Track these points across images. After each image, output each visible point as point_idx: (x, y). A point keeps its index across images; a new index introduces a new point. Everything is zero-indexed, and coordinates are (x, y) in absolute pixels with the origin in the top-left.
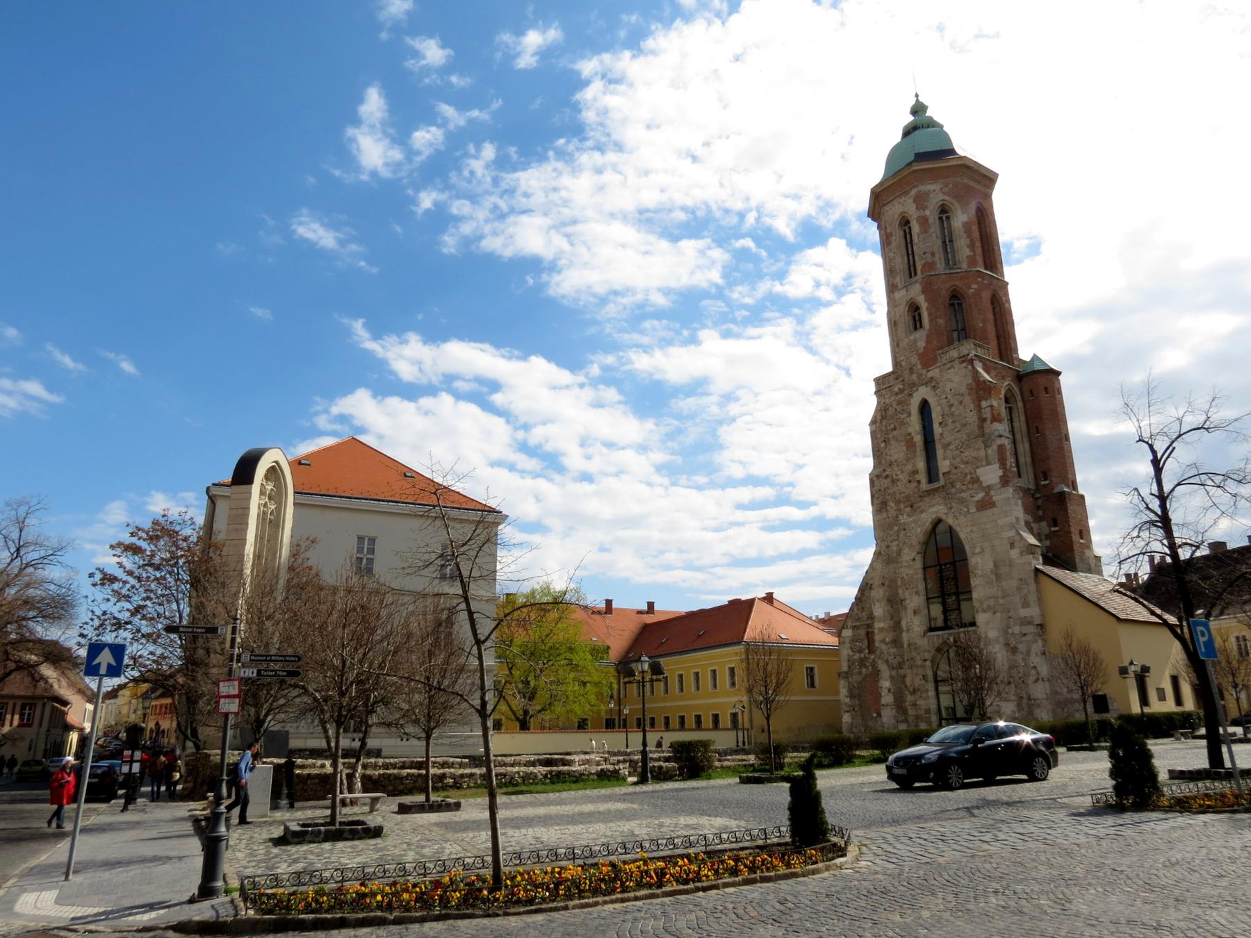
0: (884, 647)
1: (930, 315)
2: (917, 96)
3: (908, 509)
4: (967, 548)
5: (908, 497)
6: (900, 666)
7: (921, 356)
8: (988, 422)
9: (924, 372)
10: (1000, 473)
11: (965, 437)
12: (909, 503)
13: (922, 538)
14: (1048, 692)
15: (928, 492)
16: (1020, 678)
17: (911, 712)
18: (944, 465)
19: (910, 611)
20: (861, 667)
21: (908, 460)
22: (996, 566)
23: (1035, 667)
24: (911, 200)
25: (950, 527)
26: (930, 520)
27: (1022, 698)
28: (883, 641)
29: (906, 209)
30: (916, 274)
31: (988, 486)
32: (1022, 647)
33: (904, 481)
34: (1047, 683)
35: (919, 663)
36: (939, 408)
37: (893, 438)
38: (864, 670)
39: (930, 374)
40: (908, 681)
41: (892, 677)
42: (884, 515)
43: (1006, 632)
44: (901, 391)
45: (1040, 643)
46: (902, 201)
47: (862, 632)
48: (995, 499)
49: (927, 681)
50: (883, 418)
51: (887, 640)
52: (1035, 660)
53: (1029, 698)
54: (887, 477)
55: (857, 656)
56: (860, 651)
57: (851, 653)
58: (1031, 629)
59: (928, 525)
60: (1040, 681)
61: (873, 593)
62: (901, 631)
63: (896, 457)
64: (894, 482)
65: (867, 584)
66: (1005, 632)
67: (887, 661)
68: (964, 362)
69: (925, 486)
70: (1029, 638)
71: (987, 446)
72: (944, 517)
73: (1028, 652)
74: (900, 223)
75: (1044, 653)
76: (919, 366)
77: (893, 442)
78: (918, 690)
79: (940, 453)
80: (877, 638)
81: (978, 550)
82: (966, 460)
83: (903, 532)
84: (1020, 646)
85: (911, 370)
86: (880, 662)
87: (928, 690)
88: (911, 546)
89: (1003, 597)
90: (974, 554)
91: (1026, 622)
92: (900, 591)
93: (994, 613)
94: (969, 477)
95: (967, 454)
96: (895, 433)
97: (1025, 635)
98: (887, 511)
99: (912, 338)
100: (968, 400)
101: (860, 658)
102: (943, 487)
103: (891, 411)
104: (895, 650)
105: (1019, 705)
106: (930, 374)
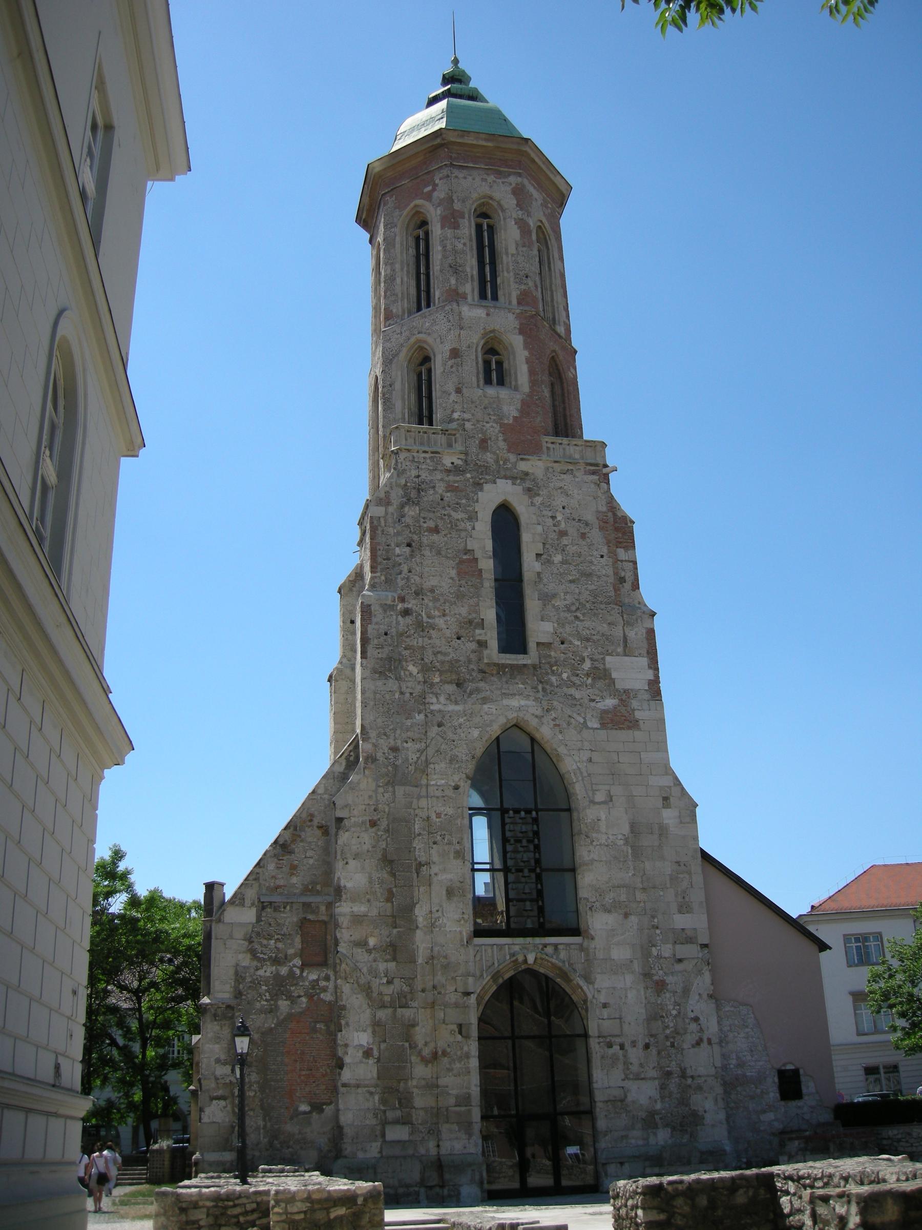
0: (361, 956)
1: (532, 372)
2: (456, 61)
3: (451, 688)
4: (579, 790)
5: (453, 666)
6: (402, 1001)
7: (506, 429)
8: (628, 586)
9: (512, 457)
10: (650, 675)
11: (585, 595)
12: (454, 677)
13: (479, 751)
14: (718, 1064)
15: (501, 668)
16: (667, 1037)
17: (421, 1101)
19: (438, 892)
20: (275, 997)
21: (460, 596)
22: (633, 827)
23: (696, 1019)
24: (509, 189)
25: (533, 740)
26: (502, 720)
27: (669, 1074)
28: (362, 944)
29: (497, 195)
30: (495, 297)
33: (448, 633)
34: (716, 1048)
35: (452, 998)
36: (539, 529)
37: (431, 546)
38: (284, 1005)
39: (523, 466)
40: (420, 1034)
41: (376, 1025)
42: (392, 684)
43: (646, 955)
44: (456, 470)
45: (707, 977)
46: (491, 178)
47: (289, 918)
48: (638, 715)
49: (467, 1037)
50: (408, 501)
51: (372, 942)
52: (698, 1005)
53: (683, 1075)
54: (406, 612)
55: (267, 971)
56: (276, 961)
57: (246, 960)
58: (690, 951)
59: (495, 730)
60: (705, 1044)
61: (344, 837)
62: (412, 927)
63: (433, 582)
64: (421, 626)
65: (311, 817)
66: (646, 948)
67: (367, 990)
68: (594, 473)
69: (493, 652)
70: (688, 966)
71: (627, 624)
72: (534, 722)
73: (686, 991)
74: (475, 210)
75: (711, 996)
76: (502, 444)
77: (427, 552)
78: (444, 1053)
79: (532, 605)
80: (345, 935)
81: (600, 797)
82: (585, 633)
83: (435, 729)
84: (669, 979)
85: (484, 444)
86: (346, 988)
87: (467, 1056)
88: (453, 760)
89: (644, 889)
90: (592, 802)
91: (685, 938)
92: (418, 844)
93: (626, 915)
94: (587, 665)
95: (587, 624)
96: (435, 537)
97: (680, 961)
98: (398, 678)
99: (491, 391)
100: (596, 535)
101: (277, 976)
102: (534, 667)
103: (430, 497)
104: (392, 965)
105: (663, 1087)
106: (523, 466)
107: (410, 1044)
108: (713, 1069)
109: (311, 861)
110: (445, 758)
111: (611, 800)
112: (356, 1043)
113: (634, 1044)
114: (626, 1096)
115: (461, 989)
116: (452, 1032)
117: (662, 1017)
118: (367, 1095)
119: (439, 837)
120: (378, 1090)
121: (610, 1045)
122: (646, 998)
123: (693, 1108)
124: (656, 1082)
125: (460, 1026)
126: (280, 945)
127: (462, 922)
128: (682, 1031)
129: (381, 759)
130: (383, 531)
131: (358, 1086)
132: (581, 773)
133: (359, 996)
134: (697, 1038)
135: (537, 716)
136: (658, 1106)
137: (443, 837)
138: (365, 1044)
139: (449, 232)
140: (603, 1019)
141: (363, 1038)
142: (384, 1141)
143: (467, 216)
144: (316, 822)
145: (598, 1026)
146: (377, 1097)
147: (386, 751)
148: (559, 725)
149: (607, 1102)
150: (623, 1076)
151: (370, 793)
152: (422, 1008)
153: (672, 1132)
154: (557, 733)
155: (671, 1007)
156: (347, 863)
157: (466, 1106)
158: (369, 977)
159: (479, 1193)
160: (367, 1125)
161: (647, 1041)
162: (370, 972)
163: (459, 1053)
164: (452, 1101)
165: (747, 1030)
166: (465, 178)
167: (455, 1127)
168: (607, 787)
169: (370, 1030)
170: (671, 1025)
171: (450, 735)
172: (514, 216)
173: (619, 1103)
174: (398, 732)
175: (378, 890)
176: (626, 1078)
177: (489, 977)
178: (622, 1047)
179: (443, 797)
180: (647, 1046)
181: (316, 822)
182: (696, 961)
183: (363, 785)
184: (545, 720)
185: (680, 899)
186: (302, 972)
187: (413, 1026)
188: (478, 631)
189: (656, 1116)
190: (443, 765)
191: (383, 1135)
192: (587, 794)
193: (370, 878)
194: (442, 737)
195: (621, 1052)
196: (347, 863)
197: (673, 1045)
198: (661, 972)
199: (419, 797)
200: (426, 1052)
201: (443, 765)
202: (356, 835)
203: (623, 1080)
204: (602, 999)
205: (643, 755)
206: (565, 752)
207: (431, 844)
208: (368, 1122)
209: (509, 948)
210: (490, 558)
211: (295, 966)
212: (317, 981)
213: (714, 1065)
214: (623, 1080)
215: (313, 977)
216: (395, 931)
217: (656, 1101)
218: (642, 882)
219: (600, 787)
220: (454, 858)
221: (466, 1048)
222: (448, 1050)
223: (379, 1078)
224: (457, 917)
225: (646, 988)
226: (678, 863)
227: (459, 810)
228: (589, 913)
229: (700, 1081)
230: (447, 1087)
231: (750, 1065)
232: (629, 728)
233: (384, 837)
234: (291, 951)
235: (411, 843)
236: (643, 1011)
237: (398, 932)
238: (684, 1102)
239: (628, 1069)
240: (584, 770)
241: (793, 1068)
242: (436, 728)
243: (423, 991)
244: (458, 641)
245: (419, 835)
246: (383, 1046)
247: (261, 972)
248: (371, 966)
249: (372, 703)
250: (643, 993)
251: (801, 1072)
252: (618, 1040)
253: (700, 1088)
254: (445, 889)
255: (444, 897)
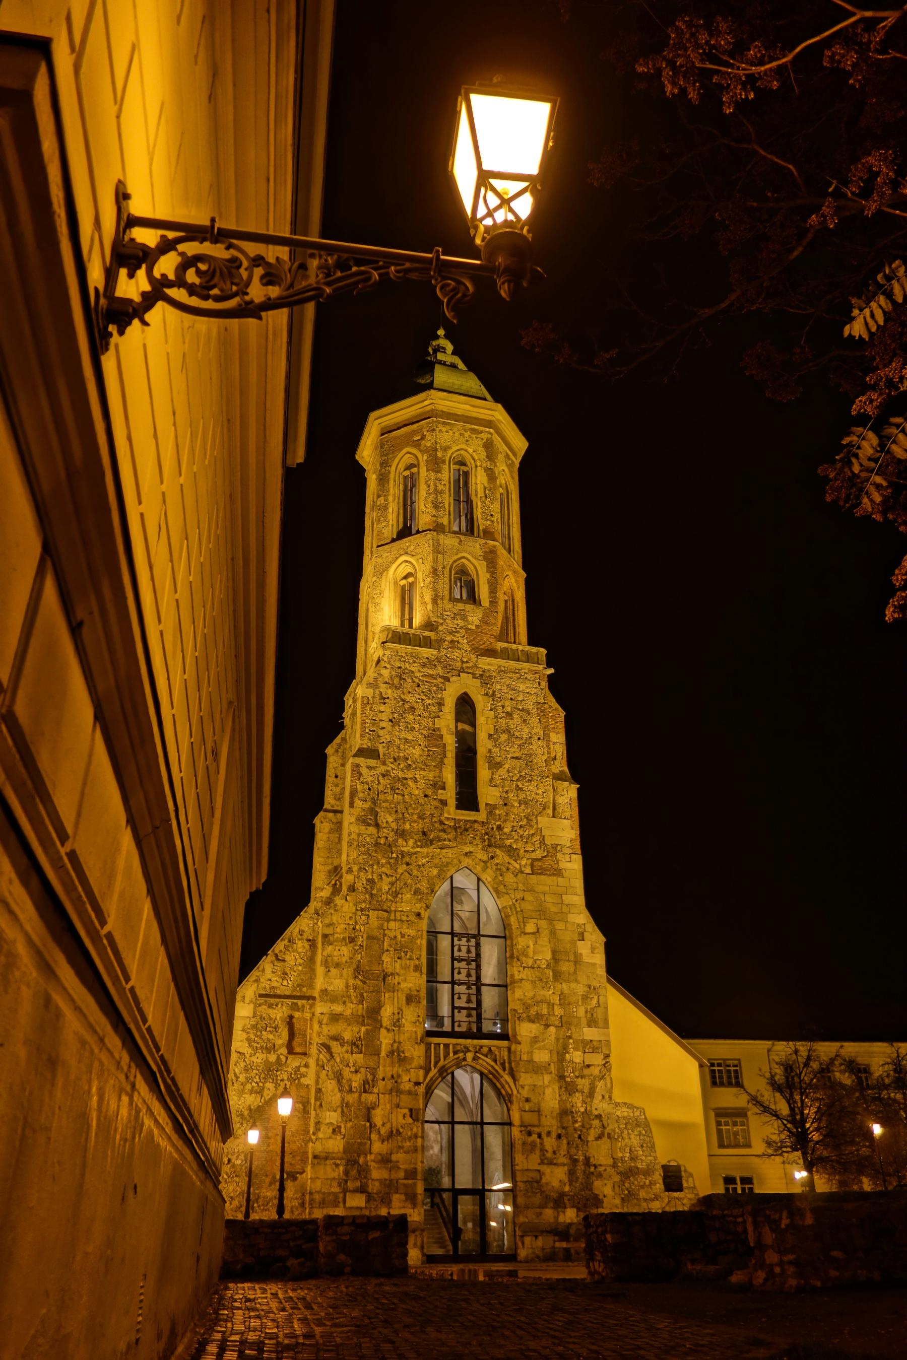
17: (377, 1174)
18: (487, 794)
23: (599, 1117)
24: (481, 443)
27: (575, 1161)
31: (555, 846)
32: (583, 1084)
35: (406, 1086)
38: (270, 1085)
40: (378, 1117)
41: (344, 1106)
42: (372, 830)
47: (279, 1013)
48: (562, 865)
60: (605, 1138)
78: (398, 1132)
79: (483, 773)
81: (530, 928)
84: (579, 1081)
92: (386, 958)
93: (547, 1026)
97: (588, 1066)
101: (267, 1062)
105: (571, 1173)
107: (371, 1124)
108: (612, 1160)
109: (300, 968)
110: (410, 890)
111: (538, 931)
112: (328, 1121)
113: (549, 1134)
114: (541, 1178)
115: (413, 1080)
116: (404, 1116)
117: (572, 1112)
118: (334, 1166)
119: (403, 954)
120: (344, 1162)
121: (530, 1134)
122: (560, 1096)
123: (596, 1192)
124: (566, 1168)
125: (411, 1110)
126: (271, 1037)
127: (417, 1024)
128: (588, 1126)
129: (360, 888)
130: (371, 708)
131: (326, 1158)
132: (516, 908)
133: (332, 1081)
134: (599, 1132)
135: (483, 862)
136: (567, 1189)
137: (406, 953)
138: (335, 1123)
139: (432, 475)
140: (525, 1111)
141: (332, 1117)
142: (345, 1206)
143: (447, 462)
144: (305, 936)
145: (521, 1116)
146: (341, 1168)
147: (365, 883)
148: (500, 869)
149: (526, 1182)
150: (539, 1161)
151: (351, 915)
152: (382, 1094)
153: (577, 1212)
154: (499, 875)
155: (579, 1105)
156: (329, 971)
157: (412, 1179)
158: (341, 1066)
159: (420, 1256)
160: (332, 1192)
161: (560, 1132)
162: (342, 1062)
163: (409, 1133)
164: (402, 1174)
165: (639, 1129)
166: (447, 432)
167: (403, 1197)
168: (535, 921)
169: (339, 1110)
170: (579, 1120)
171: (415, 872)
172: (484, 465)
173: (535, 1184)
174: (375, 867)
175: (352, 994)
176: (542, 1163)
177: (436, 1070)
178: (540, 1136)
179: (407, 921)
180: (559, 1137)
181: (305, 936)
182: (600, 1067)
183: (344, 909)
184: (489, 865)
185: (589, 1015)
186: (287, 1058)
187: (374, 1108)
188: (440, 791)
189: (565, 1198)
190: (408, 896)
191: (345, 1202)
192: (519, 925)
193: (347, 984)
194: (409, 874)
195: (538, 1140)
196: (329, 971)
197: (580, 1137)
198: (572, 1074)
199: (388, 920)
200: (383, 1131)
201: (408, 896)
202: (337, 948)
203: (539, 1164)
204: (525, 1093)
205: (564, 897)
206: (504, 890)
207: (396, 959)
208: (333, 1190)
209: (453, 1048)
210: (453, 734)
211: (282, 1054)
212: (300, 1066)
213: (612, 1156)
214: (539, 1164)
215: (297, 1064)
216: (363, 1029)
217: (565, 1184)
218: (560, 1000)
219: (531, 920)
220: (414, 971)
221: (415, 1129)
222: (401, 1130)
223: (344, 1152)
224: (414, 1019)
225: (561, 1088)
226: (590, 987)
227: (420, 933)
228: (517, 1022)
229: (601, 1169)
230: (398, 1162)
231: (641, 1159)
232: (554, 875)
233: (360, 951)
234: (279, 1042)
235: (381, 958)
236: (557, 1106)
237: (367, 1029)
238: (588, 1186)
239: (544, 1155)
240: (517, 906)
241: (676, 1164)
242: (405, 866)
243: (383, 1079)
244: (426, 799)
245: (387, 951)
246: (349, 1125)
247: (254, 1059)
248: (343, 1057)
249: (356, 843)
250: (557, 1091)
251: (683, 1169)
252: (536, 1130)
253: (600, 1176)
254: (405, 995)
255: (404, 1003)
